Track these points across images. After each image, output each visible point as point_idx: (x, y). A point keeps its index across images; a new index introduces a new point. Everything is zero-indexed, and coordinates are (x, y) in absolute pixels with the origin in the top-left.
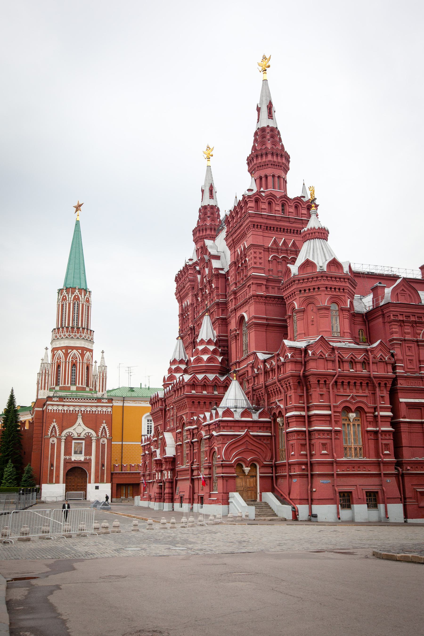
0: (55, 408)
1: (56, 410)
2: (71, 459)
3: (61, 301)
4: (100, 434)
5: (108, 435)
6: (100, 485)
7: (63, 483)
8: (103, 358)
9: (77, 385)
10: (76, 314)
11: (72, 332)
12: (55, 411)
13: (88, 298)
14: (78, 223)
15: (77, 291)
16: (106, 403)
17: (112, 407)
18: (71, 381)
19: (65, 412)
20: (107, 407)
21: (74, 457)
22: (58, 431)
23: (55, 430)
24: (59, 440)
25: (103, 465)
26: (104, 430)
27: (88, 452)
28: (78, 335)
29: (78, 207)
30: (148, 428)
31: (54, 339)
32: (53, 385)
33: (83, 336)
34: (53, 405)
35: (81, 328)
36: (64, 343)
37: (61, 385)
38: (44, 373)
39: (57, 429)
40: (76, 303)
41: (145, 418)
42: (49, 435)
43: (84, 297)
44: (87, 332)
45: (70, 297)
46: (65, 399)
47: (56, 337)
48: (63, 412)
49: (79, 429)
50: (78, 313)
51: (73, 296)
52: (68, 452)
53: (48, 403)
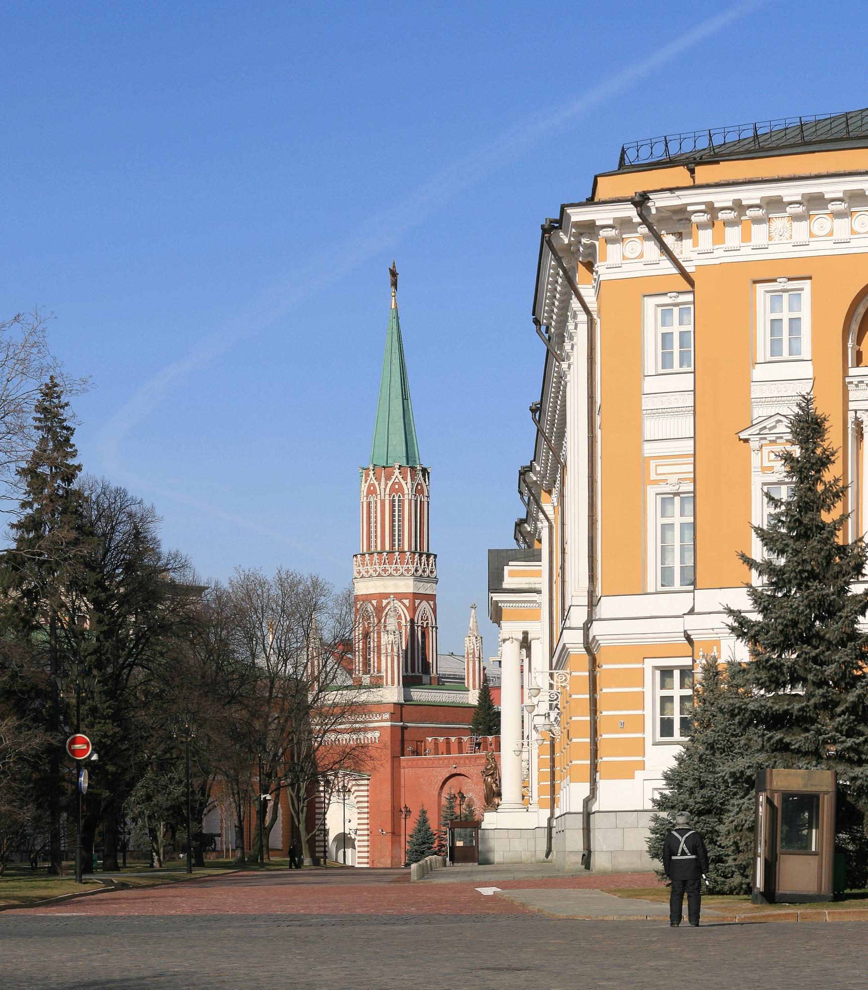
44: (428, 560)
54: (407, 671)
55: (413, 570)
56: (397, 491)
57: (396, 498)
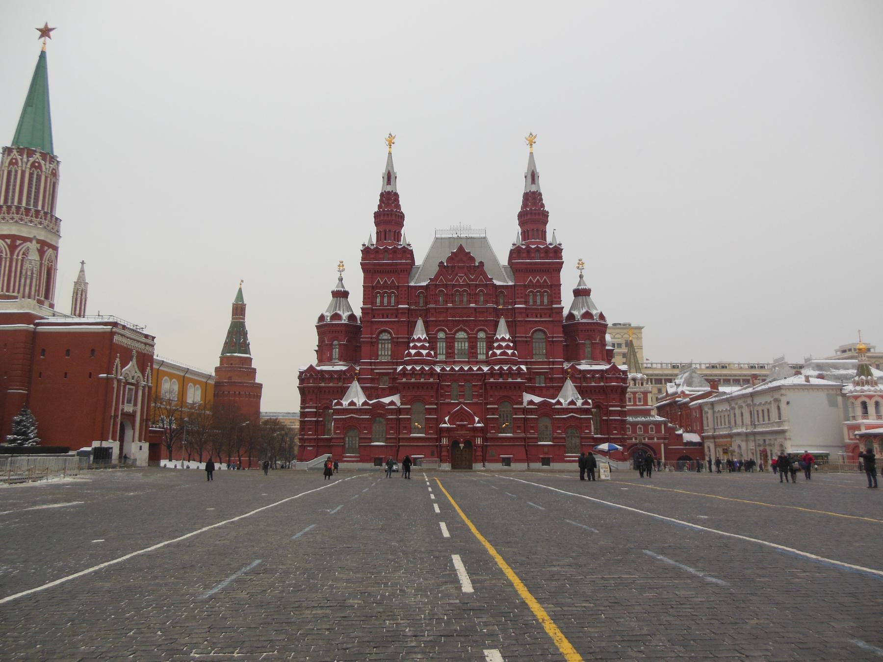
3: (29, 166)
8: (82, 271)
14: (43, 56)
29: (45, 32)
49: (131, 369)
56: (36, 168)
57: (35, 173)
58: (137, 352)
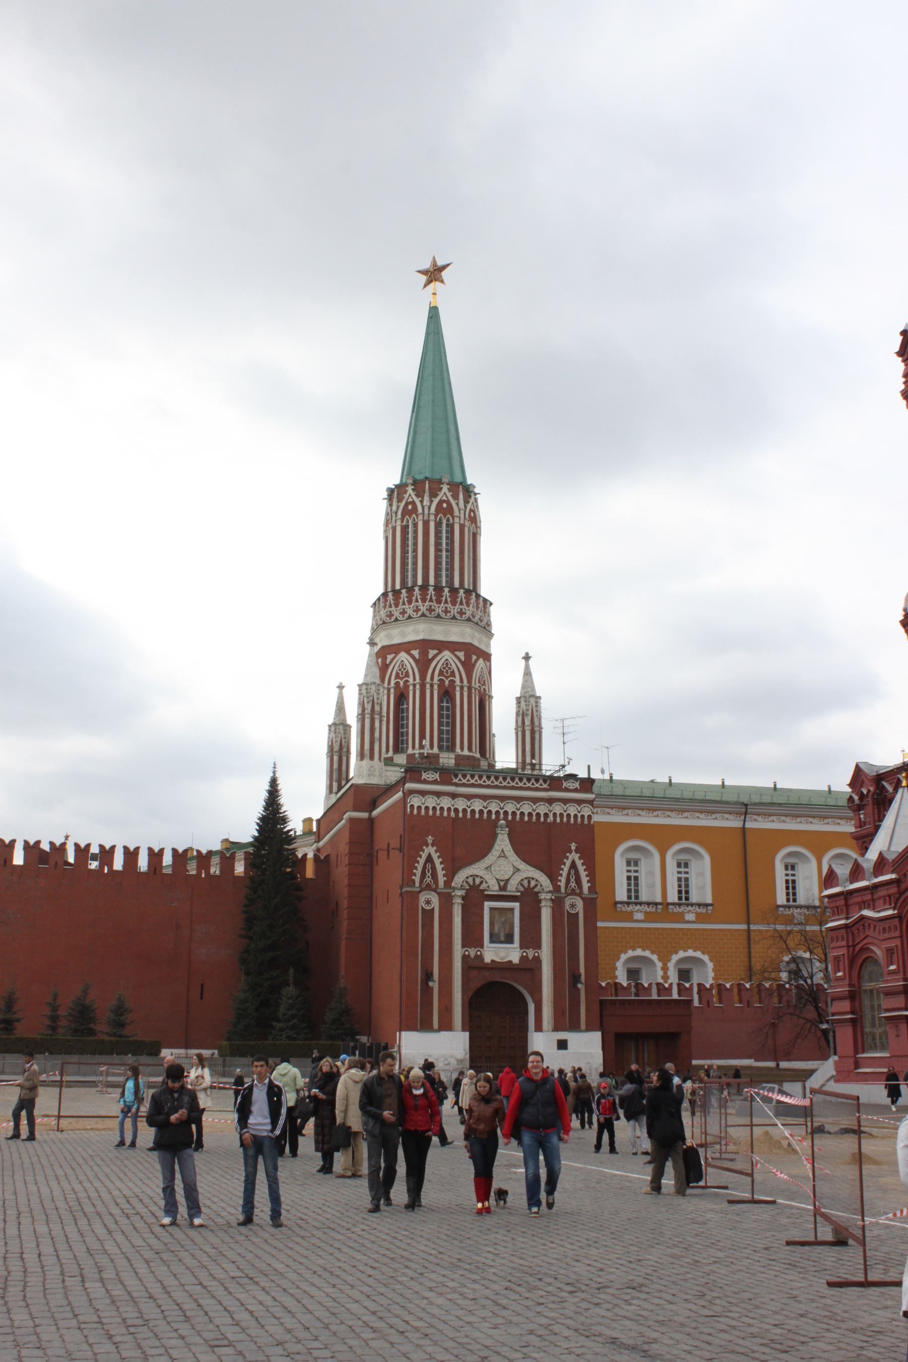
0: (431, 802)
1: (434, 808)
2: (480, 958)
3: (399, 516)
4: (562, 884)
5: (586, 886)
6: (572, 1037)
7: (464, 1030)
8: (527, 673)
9: (458, 750)
10: (444, 554)
11: (439, 602)
12: (431, 813)
13: (474, 512)
14: (434, 314)
15: (445, 488)
16: (575, 790)
17: (591, 802)
18: (440, 740)
19: (461, 815)
20: (579, 802)
21: (492, 953)
22: (440, 873)
23: (434, 868)
24: (446, 900)
25: (575, 978)
26: (573, 872)
27: (531, 939)
28: (455, 610)
29: (434, 274)
30: (629, 885)
31: (384, 623)
32: (387, 751)
33: (469, 614)
34: (423, 793)
35: (462, 591)
36: (417, 632)
37: (410, 751)
38: (368, 711)
39: (439, 867)
40: (444, 522)
41: (622, 855)
42: (417, 884)
43: (466, 507)
45: (427, 506)
46: (456, 776)
47: (390, 615)
48: (453, 814)
50: (450, 551)
51: (436, 501)
52: (472, 938)
53: (409, 786)
54: (414, 747)
55: (423, 609)
58: (509, 824)
